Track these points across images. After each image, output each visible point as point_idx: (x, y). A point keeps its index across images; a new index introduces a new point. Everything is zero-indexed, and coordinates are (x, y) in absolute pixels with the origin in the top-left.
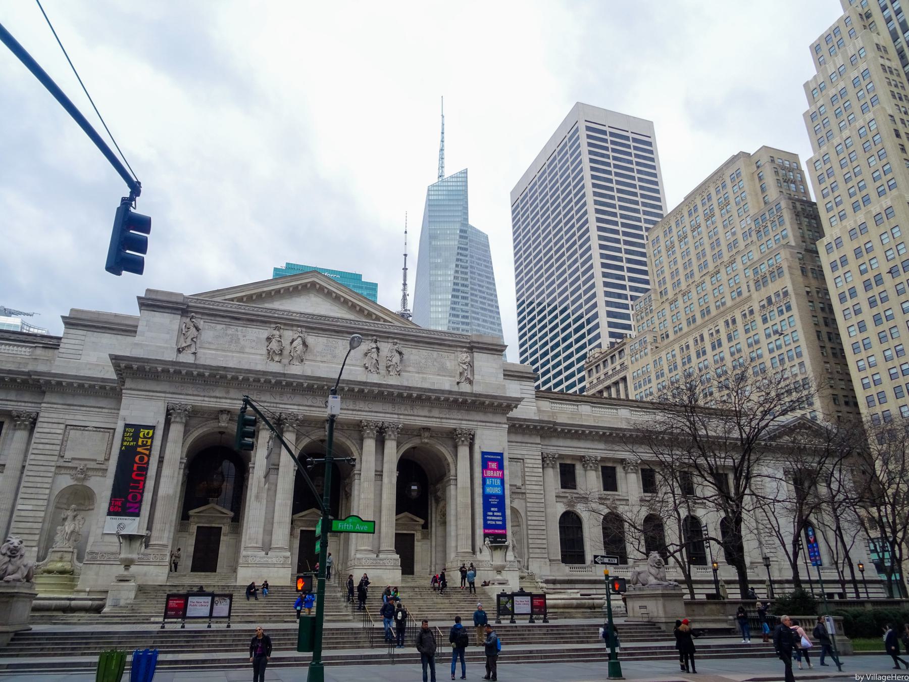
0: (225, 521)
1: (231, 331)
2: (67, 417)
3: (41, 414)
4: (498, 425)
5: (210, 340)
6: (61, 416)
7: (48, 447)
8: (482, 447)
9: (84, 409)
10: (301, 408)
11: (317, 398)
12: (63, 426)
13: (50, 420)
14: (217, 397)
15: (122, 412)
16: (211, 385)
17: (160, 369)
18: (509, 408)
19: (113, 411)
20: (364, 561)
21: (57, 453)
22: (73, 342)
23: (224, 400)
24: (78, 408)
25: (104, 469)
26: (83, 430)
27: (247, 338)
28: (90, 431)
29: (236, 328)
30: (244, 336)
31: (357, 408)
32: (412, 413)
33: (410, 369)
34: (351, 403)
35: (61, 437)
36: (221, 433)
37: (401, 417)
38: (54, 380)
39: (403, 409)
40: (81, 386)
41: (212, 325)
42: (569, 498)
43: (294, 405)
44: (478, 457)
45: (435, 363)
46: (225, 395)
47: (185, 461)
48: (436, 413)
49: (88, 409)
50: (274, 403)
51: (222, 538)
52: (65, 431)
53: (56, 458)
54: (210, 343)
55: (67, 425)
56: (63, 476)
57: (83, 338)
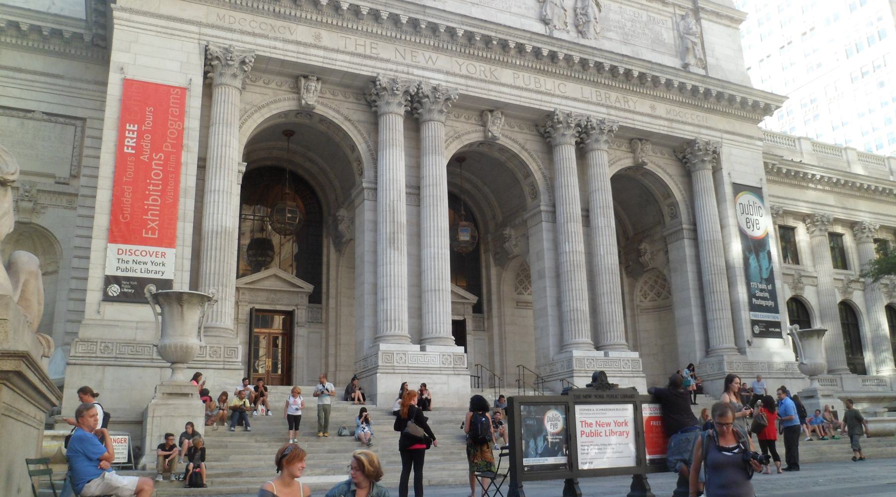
4: (749, 141)
8: (732, 175)
9: (23, 76)
10: (450, 79)
11: (477, 64)
14: (298, 43)
15: (116, 57)
18: (767, 110)
19: (79, 85)
20: (558, 366)
23: (313, 51)
25: (70, 194)
26: (24, 118)
31: (543, 89)
32: (627, 107)
33: (610, 35)
34: (532, 80)
36: (289, 133)
37: (613, 112)
39: (613, 95)
42: (796, 276)
43: (439, 71)
44: (728, 190)
45: (647, 31)
46: (313, 42)
47: (244, 169)
48: (662, 109)
50: (402, 64)
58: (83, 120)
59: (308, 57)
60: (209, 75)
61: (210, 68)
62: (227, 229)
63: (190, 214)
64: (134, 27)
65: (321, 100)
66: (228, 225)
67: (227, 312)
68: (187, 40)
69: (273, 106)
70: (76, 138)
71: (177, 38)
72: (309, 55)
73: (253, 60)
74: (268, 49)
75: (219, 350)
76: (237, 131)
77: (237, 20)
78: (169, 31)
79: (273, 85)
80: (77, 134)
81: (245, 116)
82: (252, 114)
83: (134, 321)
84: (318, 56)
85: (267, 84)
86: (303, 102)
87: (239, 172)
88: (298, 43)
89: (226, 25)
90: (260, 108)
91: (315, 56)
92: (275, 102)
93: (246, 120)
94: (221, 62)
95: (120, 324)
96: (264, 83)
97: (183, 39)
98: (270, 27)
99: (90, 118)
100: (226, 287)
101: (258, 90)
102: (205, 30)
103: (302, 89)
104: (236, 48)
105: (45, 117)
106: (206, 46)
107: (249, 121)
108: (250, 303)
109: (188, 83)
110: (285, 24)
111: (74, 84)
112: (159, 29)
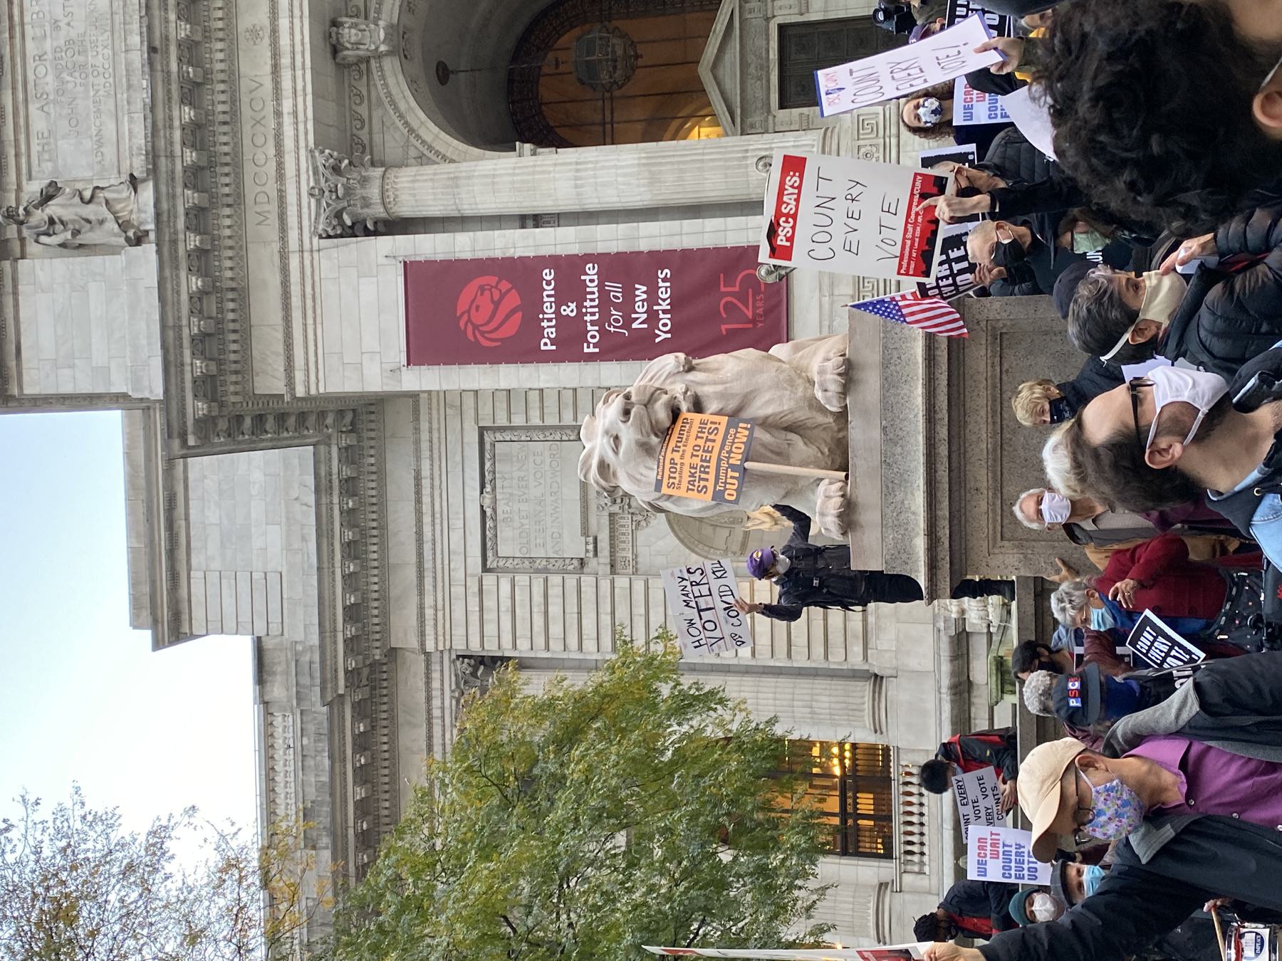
0: (755, 20)
1: (42, 76)
2: (459, 575)
3: (459, 646)
5: (88, 144)
6: (458, 590)
7: (555, 610)
12: (489, 580)
13: (474, 618)
14: (276, 69)
15: (374, 381)
16: (234, 101)
17: (196, 283)
19: (425, 445)
21: (571, 581)
22: (228, 602)
23: (284, 41)
24: (427, 547)
26: (494, 519)
27: (58, 12)
28: (495, 500)
29: (31, 64)
30: (56, 26)
35: (522, 579)
36: (443, 73)
38: (343, 629)
40: (353, 550)
41: (35, 148)
46: (267, 41)
47: (528, 147)
49: (427, 519)
51: (814, 16)
52: (505, 570)
53: (588, 581)
54: (100, 143)
55: (485, 569)
56: (641, 550)
57: (213, 578)
58: (482, 431)
59: (298, 48)
60: (370, 226)
61: (358, 228)
62: (644, 161)
63: (622, 229)
64: (317, 362)
65: (372, 15)
66: (636, 162)
67: (792, 144)
68: (317, 273)
69: (402, 106)
70: (514, 439)
71: (317, 290)
72: (293, 46)
73: (327, 151)
74: (301, 127)
75: (863, 150)
76: (464, 166)
77: (259, 189)
78: (309, 303)
79: (363, 110)
80: (508, 439)
81: (430, 155)
82: (424, 142)
83: (820, 302)
84: (292, 28)
85: (363, 122)
86: (383, 48)
87: (534, 154)
88: (276, 69)
89: (274, 207)
90: (411, 131)
91: (292, 34)
92: (393, 103)
93: (438, 153)
94: (344, 208)
95: (826, 323)
96: (362, 128)
97: (317, 279)
98: (259, 128)
99: (477, 421)
100: (747, 151)
101: (377, 138)
102: (293, 243)
103: (361, 53)
104: (312, 184)
105: (488, 488)
106: (321, 237)
107: (437, 148)
108: (769, 111)
109: (393, 261)
110: (245, 99)
111: (425, 453)
112: (310, 321)
